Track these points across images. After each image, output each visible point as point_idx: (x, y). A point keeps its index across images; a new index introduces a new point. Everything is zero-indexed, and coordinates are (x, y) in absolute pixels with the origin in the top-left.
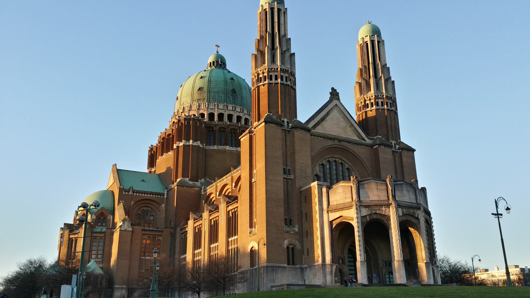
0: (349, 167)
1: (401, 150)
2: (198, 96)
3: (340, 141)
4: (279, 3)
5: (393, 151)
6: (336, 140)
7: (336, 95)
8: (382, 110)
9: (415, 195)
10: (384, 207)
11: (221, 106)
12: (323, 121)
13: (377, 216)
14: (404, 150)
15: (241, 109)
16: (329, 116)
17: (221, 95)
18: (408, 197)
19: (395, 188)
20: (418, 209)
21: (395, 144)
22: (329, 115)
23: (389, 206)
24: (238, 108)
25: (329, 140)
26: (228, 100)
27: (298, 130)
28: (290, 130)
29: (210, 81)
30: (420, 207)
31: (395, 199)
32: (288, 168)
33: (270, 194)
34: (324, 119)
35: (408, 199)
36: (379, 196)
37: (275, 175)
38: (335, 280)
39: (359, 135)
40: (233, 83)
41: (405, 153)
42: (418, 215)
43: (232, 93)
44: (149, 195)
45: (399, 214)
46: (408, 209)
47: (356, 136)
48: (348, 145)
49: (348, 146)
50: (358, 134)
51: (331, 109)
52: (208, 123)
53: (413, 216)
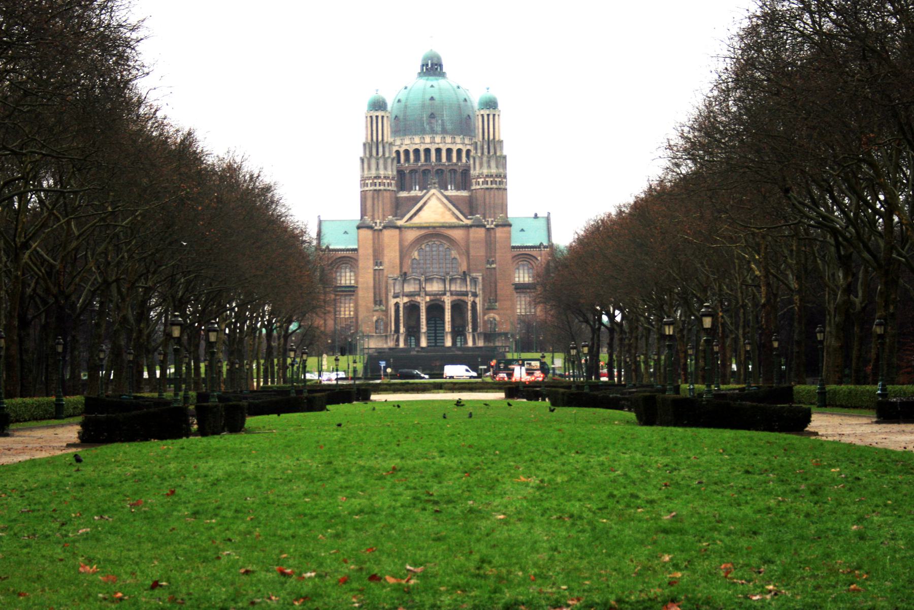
3: (434, 227)
29: (406, 107)
39: (458, 218)
51: (429, 199)
53: (439, 300)
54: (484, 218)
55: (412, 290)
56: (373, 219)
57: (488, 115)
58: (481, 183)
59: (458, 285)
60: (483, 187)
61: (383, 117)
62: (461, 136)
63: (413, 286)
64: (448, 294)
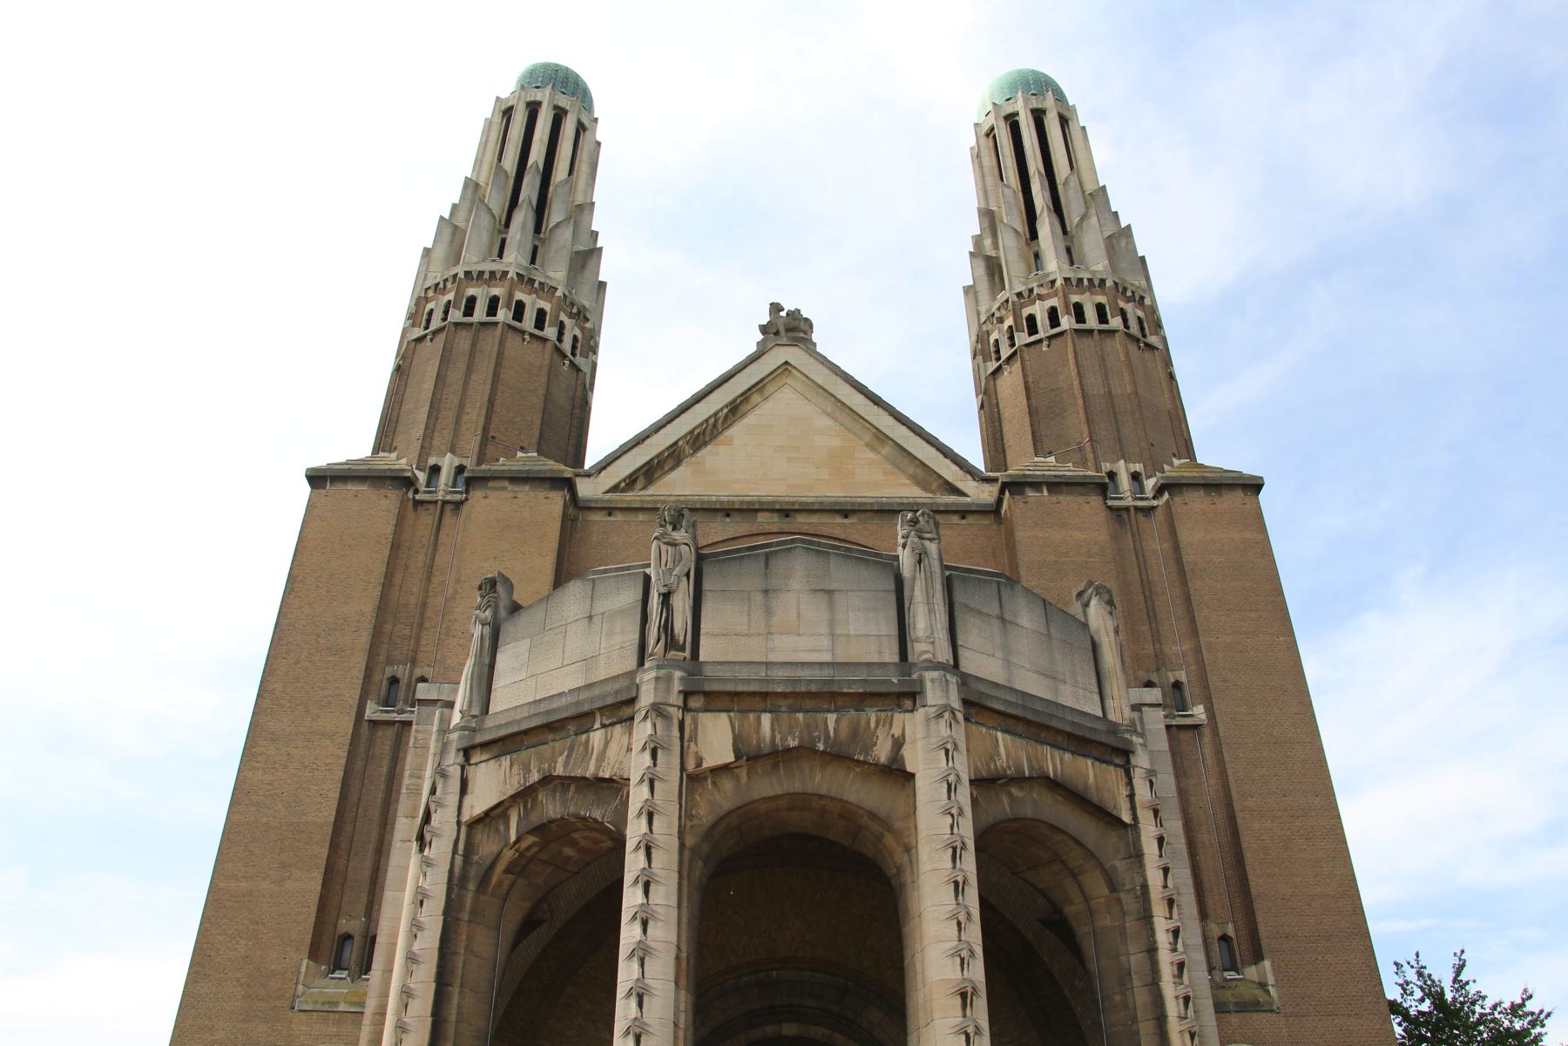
1: (1166, 496)
3: (786, 512)
4: (537, 87)
5: (1127, 509)
6: (759, 514)
8: (1054, 342)
9: (893, 613)
10: (597, 725)
12: (706, 444)
13: (564, 802)
14: (1185, 489)
16: (750, 420)
18: (825, 630)
19: (707, 585)
20: (908, 703)
21: (1135, 477)
22: (744, 415)
23: (626, 712)
25: (719, 518)
27: (491, 488)
28: (458, 497)
30: (921, 682)
33: (253, 809)
34: (713, 437)
35: (825, 642)
37: (307, 711)
42: (898, 744)
45: (705, 755)
46: (800, 716)
48: (844, 526)
49: (837, 533)
50: (919, 471)
51: (759, 386)
57: (1038, 116)
58: (1042, 320)
63: (577, 642)
64: (938, 692)
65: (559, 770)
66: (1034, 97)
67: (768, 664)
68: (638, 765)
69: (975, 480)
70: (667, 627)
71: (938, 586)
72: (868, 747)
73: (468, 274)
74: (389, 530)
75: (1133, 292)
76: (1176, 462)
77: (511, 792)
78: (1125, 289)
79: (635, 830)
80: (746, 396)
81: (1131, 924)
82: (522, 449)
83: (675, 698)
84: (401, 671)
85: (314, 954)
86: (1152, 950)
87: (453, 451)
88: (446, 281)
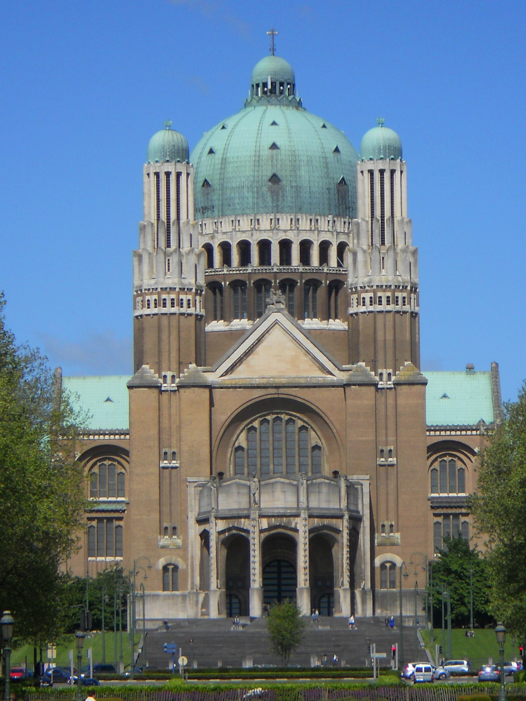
0: (305, 424)
2: (202, 199)
3: (277, 387)
4: (168, 161)
7: (277, 302)
11: (245, 224)
15: (291, 220)
17: (246, 194)
19: (262, 490)
21: (389, 374)
24: (285, 220)
26: (261, 204)
29: (224, 161)
31: (259, 507)
32: (175, 450)
36: (239, 503)
38: (202, 612)
39: (323, 368)
40: (275, 157)
41: (405, 388)
42: (296, 524)
43: (270, 184)
44: (107, 437)
47: (317, 369)
48: (295, 391)
51: (267, 331)
52: (211, 272)
54: (374, 369)
55: (235, 506)
56: (159, 371)
59: (323, 496)
60: (371, 308)
61: (179, 175)
62: (330, 217)
64: (304, 514)
65: (236, 525)
66: (380, 161)
67: (273, 508)
68: (251, 529)
69: (338, 369)
70: (255, 501)
71: (305, 490)
72: (291, 524)
73: (161, 289)
74: (157, 405)
75: (403, 286)
76: (406, 363)
77: (226, 528)
78: (399, 286)
79: (252, 541)
80: (263, 336)
81: (340, 550)
82: (191, 363)
83: (257, 517)
84: (167, 450)
85: (160, 535)
86: (343, 555)
87: (170, 370)
88: (153, 289)
